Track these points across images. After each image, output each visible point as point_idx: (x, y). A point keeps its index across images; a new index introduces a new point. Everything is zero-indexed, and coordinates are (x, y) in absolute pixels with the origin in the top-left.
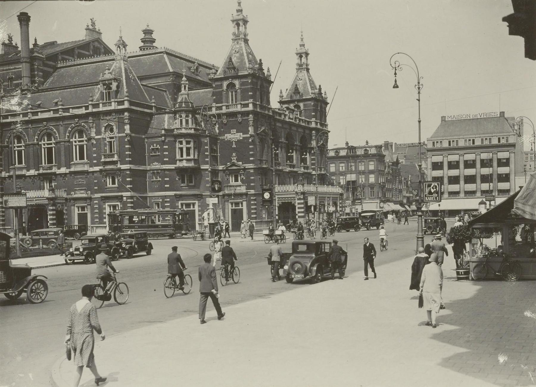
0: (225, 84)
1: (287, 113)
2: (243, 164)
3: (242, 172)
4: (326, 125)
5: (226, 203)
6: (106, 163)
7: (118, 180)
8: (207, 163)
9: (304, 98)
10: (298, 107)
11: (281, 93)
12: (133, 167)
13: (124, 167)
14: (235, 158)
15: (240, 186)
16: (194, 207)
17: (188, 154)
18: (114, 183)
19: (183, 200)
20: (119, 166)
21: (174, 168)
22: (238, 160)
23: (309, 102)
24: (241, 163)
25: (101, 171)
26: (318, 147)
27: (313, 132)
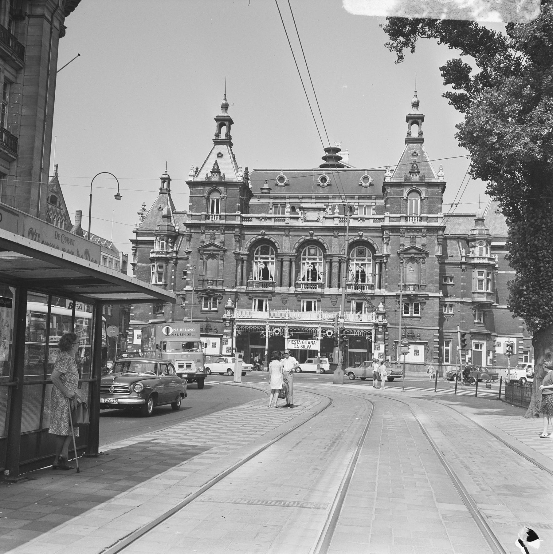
1: (299, 215)
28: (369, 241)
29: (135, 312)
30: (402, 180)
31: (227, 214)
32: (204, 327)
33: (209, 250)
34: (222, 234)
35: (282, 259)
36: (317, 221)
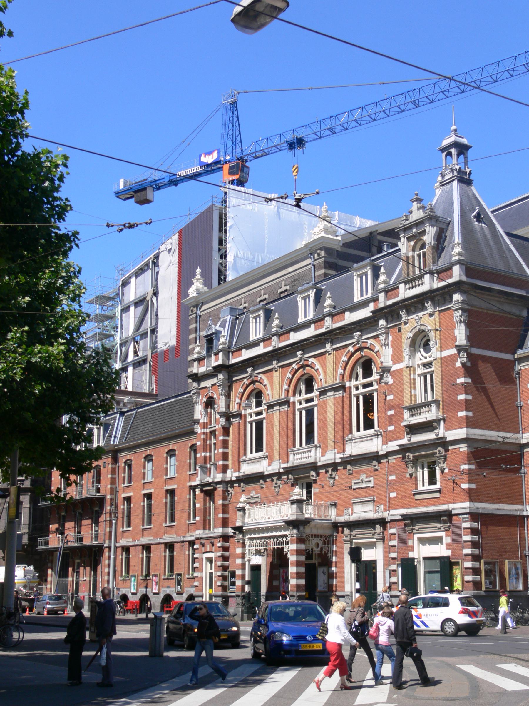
6: (413, 429)
7: (442, 471)
12: (478, 433)
13: (452, 435)
18: (432, 480)
20: (441, 431)
25: (404, 450)
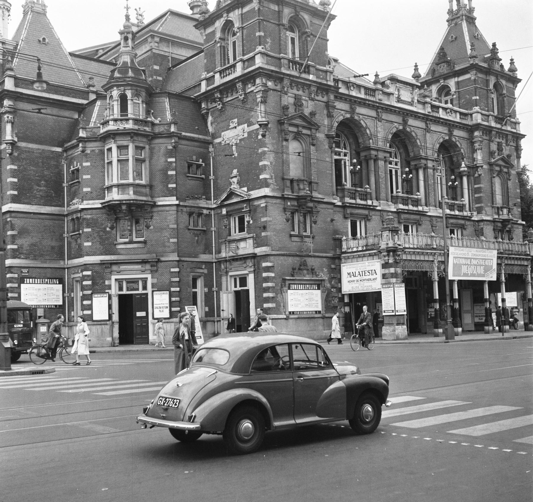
0: (219, 24)
1: (391, 90)
2: (249, 190)
3: (245, 208)
4: (517, 123)
5: (224, 279)
8: (170, 193)
9: (457, 68)
10: (444, 91)
11: (416, 69)
14: (235, 180)
15: (244, 239)
16: (145, 288)
17: (124, 174)
19: (119, 272)
21: (100, 206)
22: (241, 184)
23: (467, 76)
24: (245, 189)
26: (490, 164)
27: (476, 133)
28: (457, 143)
29: (19, 241)
30: (485, 65)
31: (318, 67)
32: (297, 266)
33: (297, 126)
34: (313, 100)
35: (376, 156)
36: (411, 104)
